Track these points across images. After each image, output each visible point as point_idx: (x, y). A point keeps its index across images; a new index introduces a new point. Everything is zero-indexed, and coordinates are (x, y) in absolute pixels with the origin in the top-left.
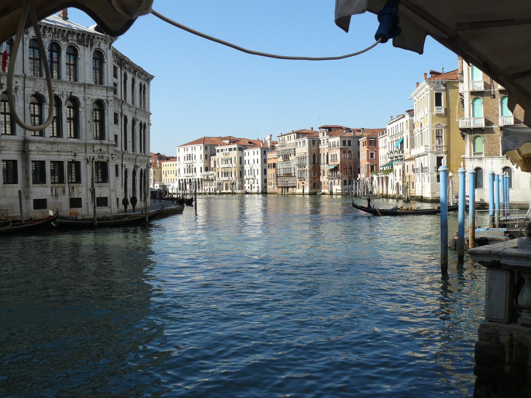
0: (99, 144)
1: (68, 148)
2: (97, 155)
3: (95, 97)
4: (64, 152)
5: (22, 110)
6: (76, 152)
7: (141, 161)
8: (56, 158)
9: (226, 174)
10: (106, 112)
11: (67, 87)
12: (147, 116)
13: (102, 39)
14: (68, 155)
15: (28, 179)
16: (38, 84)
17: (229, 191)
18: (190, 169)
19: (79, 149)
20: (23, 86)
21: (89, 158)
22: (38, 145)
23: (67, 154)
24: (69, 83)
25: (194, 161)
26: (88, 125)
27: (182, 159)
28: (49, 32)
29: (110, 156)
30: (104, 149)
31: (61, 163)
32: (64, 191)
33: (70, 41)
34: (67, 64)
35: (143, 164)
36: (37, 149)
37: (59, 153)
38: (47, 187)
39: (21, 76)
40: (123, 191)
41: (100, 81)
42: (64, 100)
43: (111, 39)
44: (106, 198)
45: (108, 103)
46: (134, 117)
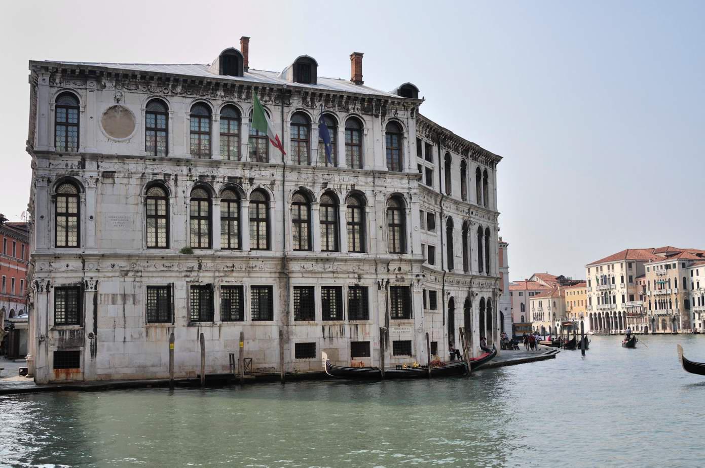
0: (398, 260)
1: (350, 267)
2: (394, 277)
3: (391, 190)
4: (342, 273)
5: (280, 215)
6: (361, 272)
7: (481, 286)
8: (330, 282)
9: (662, 305)
10: (407, 211)
11: (346, 178)
12: (492, 218)
13: (399, 103)
14: (349, 278)
15: (288, 313)
16: (304, 176)
17: (668, 331)
18: (607, 298)
19: (366, 267)
20: (282, 179)
21: (380, 281)
22: (303, 263)
23: (346, 276)
24: (349, 171)
25: (613, 286)
26: (380, 232)
27: (594, 283)
28: (319, 101)
29: (414, 277)
30: (405, 267)
31: (338, 289)
32: (342, 333)
33: (352, 111)
34: (347, 144)
35: (485, 290)
36: (302, 270)
37: (335, 275)
38: (317, 325)
39: (279, 166)
40: (446, 332)
41: (396, 163)
42: (342, 197)
43: (412, 103)
44: (408, 343)
45: (411, 198)
46: (466, 218)
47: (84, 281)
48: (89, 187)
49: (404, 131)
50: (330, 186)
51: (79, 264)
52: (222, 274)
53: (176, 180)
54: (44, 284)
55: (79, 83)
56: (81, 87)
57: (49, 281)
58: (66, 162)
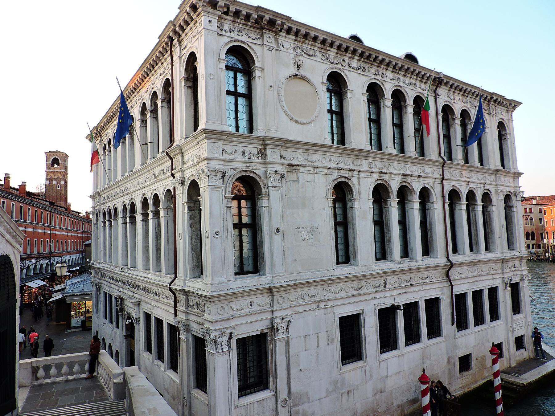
8: (477, 287)
39: (439, 162)
47: (275, 324)
48: (274, 187)
49: (508, 131)
50: (471, 185)
51: (265, 299)
52: (404, 290)
53: (359, 178)
54: (225, 339)
55: (253, 36)
56: (255, 41)
57: (231, 333)
58: (243, 148)
